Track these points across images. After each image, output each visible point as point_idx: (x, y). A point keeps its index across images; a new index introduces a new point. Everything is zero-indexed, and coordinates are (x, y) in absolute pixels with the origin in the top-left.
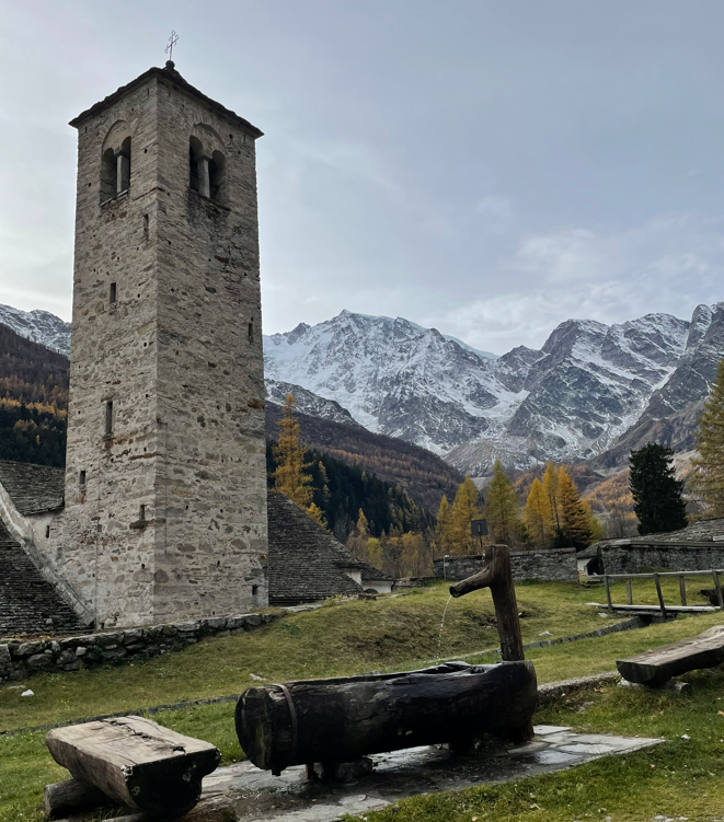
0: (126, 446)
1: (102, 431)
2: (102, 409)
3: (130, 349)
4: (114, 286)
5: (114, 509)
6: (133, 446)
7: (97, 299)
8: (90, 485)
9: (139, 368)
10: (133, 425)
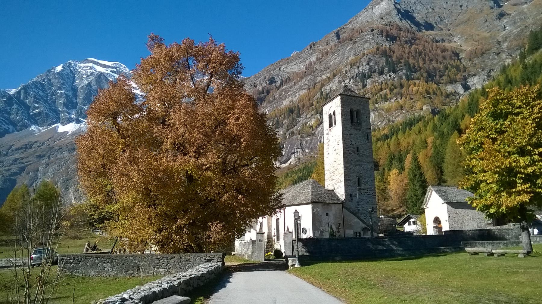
0: (366, 191)
1: (357, 184)
2: (356, 179)
3: (365, 166)
4: (357, 148)
5: (363, 206)
8: (354, 198)
9: (368, 172)
10: (367, 186)
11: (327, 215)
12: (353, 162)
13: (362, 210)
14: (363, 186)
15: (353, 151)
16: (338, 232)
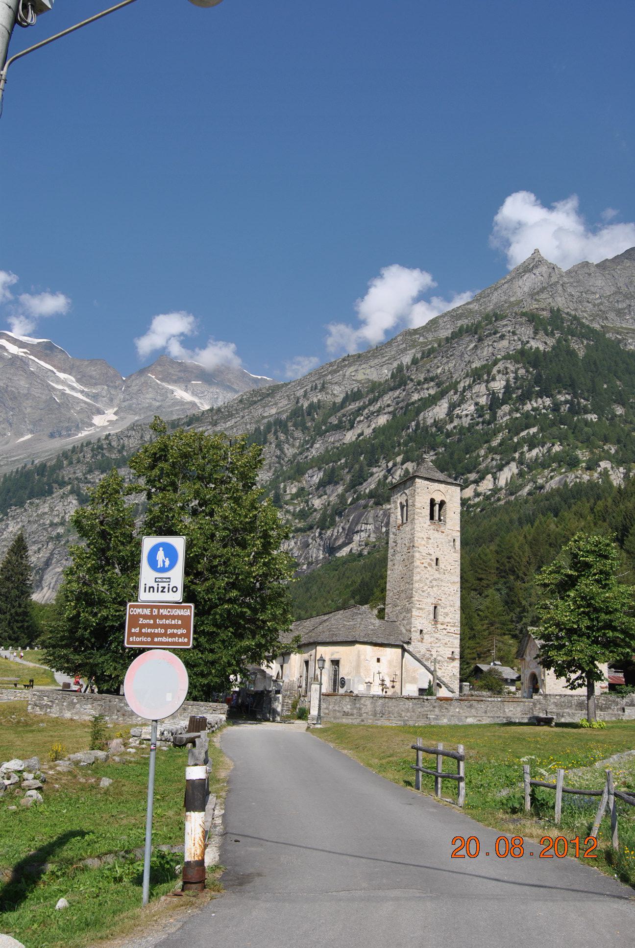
0: (445, 626)
1: (432, 616)
2: (432, 608)
3: (446, 589)
4: (437, 559)
5: (439, 649)
6: (448, 628)
7: (428, 561)
8: (426, 637)
9: (450, 598)
10: (447, 620)
11: (378, 660)
12: (428, 582)
13: (438, 655)
14: (440, 618)
15: (430, 565)
16: (393, 687)
